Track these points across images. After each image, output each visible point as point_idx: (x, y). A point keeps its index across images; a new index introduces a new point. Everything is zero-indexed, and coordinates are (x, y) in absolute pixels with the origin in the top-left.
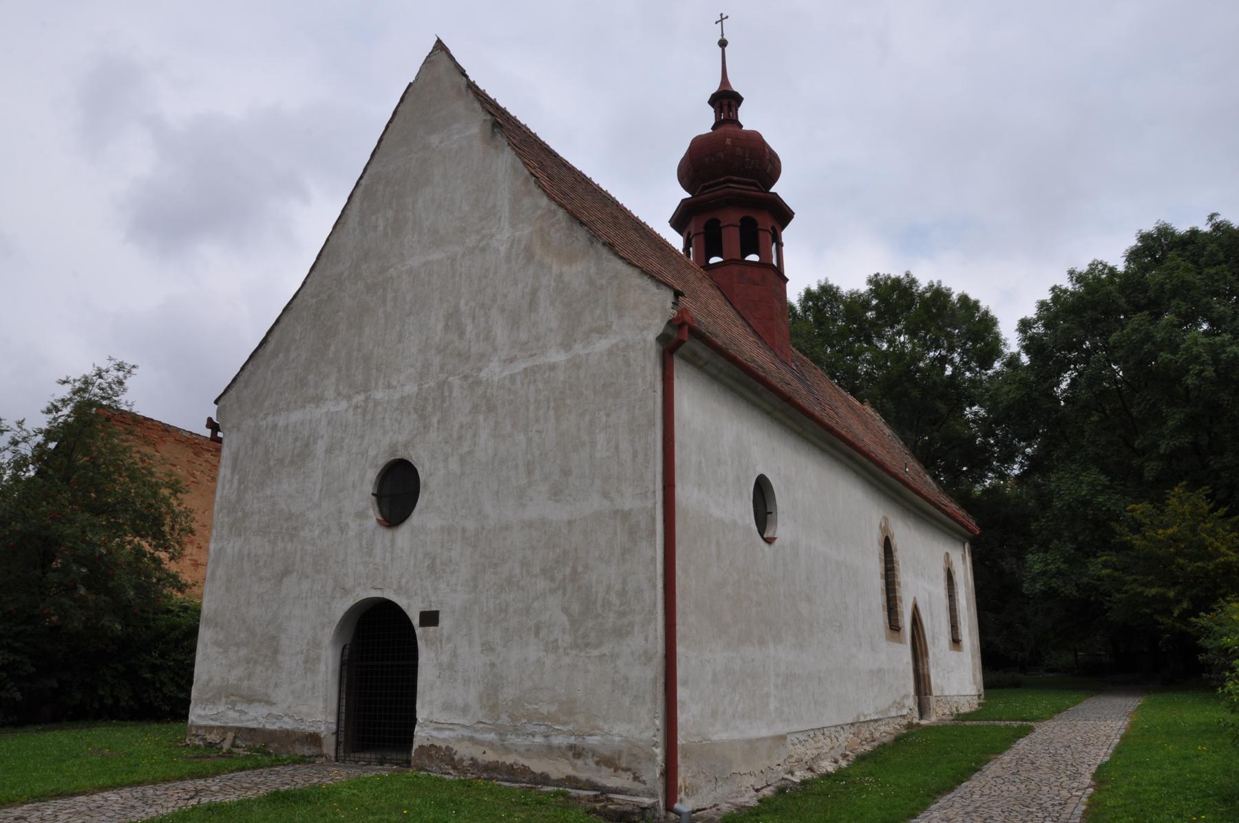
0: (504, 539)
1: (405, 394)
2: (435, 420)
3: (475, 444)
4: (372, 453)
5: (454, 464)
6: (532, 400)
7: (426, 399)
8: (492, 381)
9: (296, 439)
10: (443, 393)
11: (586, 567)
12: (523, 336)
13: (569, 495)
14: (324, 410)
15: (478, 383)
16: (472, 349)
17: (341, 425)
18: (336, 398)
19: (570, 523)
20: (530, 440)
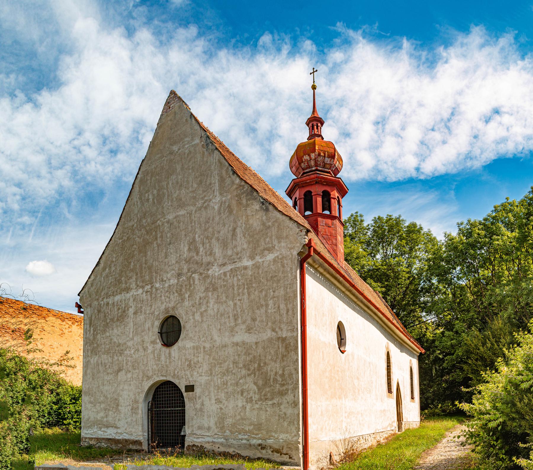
0: (224, 351)
1: (171, 284)
2: (187, 296)
3: (208, 307)
4: (156, 313)
5: (197, 317)
6: (236, 285)
7: (181, 286)
8: (215, 276)
9: (119, 309)
10: (190, 282)
11: (265, 363)
12: (230, 252)
13: (256, 330)
14: (131, 294)
15: (208, 276)
16: (203, 260)
17: (140, 300)
18: (136, 288)
19: (256, 343)
20: (235, 304)
